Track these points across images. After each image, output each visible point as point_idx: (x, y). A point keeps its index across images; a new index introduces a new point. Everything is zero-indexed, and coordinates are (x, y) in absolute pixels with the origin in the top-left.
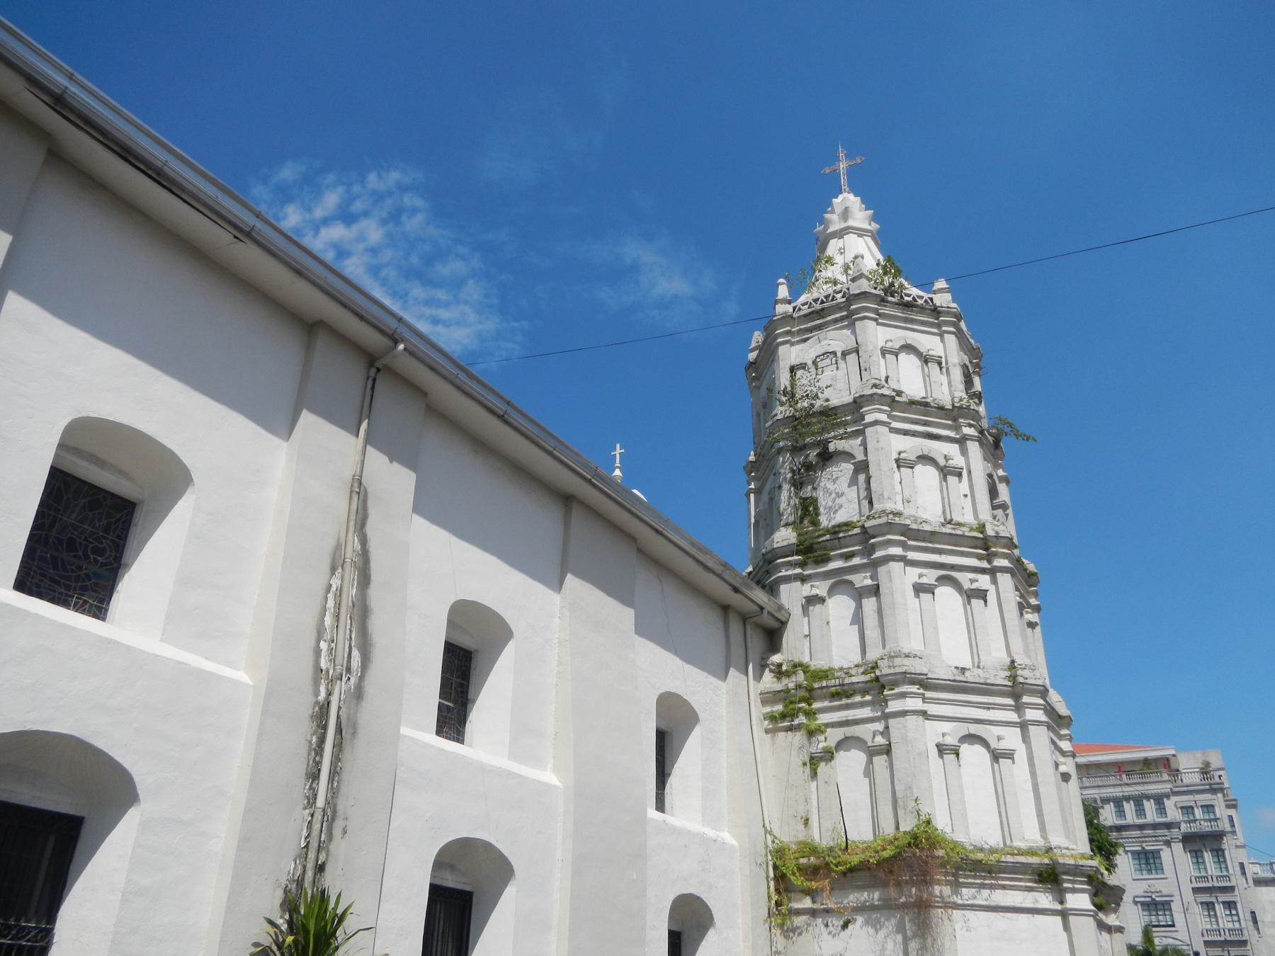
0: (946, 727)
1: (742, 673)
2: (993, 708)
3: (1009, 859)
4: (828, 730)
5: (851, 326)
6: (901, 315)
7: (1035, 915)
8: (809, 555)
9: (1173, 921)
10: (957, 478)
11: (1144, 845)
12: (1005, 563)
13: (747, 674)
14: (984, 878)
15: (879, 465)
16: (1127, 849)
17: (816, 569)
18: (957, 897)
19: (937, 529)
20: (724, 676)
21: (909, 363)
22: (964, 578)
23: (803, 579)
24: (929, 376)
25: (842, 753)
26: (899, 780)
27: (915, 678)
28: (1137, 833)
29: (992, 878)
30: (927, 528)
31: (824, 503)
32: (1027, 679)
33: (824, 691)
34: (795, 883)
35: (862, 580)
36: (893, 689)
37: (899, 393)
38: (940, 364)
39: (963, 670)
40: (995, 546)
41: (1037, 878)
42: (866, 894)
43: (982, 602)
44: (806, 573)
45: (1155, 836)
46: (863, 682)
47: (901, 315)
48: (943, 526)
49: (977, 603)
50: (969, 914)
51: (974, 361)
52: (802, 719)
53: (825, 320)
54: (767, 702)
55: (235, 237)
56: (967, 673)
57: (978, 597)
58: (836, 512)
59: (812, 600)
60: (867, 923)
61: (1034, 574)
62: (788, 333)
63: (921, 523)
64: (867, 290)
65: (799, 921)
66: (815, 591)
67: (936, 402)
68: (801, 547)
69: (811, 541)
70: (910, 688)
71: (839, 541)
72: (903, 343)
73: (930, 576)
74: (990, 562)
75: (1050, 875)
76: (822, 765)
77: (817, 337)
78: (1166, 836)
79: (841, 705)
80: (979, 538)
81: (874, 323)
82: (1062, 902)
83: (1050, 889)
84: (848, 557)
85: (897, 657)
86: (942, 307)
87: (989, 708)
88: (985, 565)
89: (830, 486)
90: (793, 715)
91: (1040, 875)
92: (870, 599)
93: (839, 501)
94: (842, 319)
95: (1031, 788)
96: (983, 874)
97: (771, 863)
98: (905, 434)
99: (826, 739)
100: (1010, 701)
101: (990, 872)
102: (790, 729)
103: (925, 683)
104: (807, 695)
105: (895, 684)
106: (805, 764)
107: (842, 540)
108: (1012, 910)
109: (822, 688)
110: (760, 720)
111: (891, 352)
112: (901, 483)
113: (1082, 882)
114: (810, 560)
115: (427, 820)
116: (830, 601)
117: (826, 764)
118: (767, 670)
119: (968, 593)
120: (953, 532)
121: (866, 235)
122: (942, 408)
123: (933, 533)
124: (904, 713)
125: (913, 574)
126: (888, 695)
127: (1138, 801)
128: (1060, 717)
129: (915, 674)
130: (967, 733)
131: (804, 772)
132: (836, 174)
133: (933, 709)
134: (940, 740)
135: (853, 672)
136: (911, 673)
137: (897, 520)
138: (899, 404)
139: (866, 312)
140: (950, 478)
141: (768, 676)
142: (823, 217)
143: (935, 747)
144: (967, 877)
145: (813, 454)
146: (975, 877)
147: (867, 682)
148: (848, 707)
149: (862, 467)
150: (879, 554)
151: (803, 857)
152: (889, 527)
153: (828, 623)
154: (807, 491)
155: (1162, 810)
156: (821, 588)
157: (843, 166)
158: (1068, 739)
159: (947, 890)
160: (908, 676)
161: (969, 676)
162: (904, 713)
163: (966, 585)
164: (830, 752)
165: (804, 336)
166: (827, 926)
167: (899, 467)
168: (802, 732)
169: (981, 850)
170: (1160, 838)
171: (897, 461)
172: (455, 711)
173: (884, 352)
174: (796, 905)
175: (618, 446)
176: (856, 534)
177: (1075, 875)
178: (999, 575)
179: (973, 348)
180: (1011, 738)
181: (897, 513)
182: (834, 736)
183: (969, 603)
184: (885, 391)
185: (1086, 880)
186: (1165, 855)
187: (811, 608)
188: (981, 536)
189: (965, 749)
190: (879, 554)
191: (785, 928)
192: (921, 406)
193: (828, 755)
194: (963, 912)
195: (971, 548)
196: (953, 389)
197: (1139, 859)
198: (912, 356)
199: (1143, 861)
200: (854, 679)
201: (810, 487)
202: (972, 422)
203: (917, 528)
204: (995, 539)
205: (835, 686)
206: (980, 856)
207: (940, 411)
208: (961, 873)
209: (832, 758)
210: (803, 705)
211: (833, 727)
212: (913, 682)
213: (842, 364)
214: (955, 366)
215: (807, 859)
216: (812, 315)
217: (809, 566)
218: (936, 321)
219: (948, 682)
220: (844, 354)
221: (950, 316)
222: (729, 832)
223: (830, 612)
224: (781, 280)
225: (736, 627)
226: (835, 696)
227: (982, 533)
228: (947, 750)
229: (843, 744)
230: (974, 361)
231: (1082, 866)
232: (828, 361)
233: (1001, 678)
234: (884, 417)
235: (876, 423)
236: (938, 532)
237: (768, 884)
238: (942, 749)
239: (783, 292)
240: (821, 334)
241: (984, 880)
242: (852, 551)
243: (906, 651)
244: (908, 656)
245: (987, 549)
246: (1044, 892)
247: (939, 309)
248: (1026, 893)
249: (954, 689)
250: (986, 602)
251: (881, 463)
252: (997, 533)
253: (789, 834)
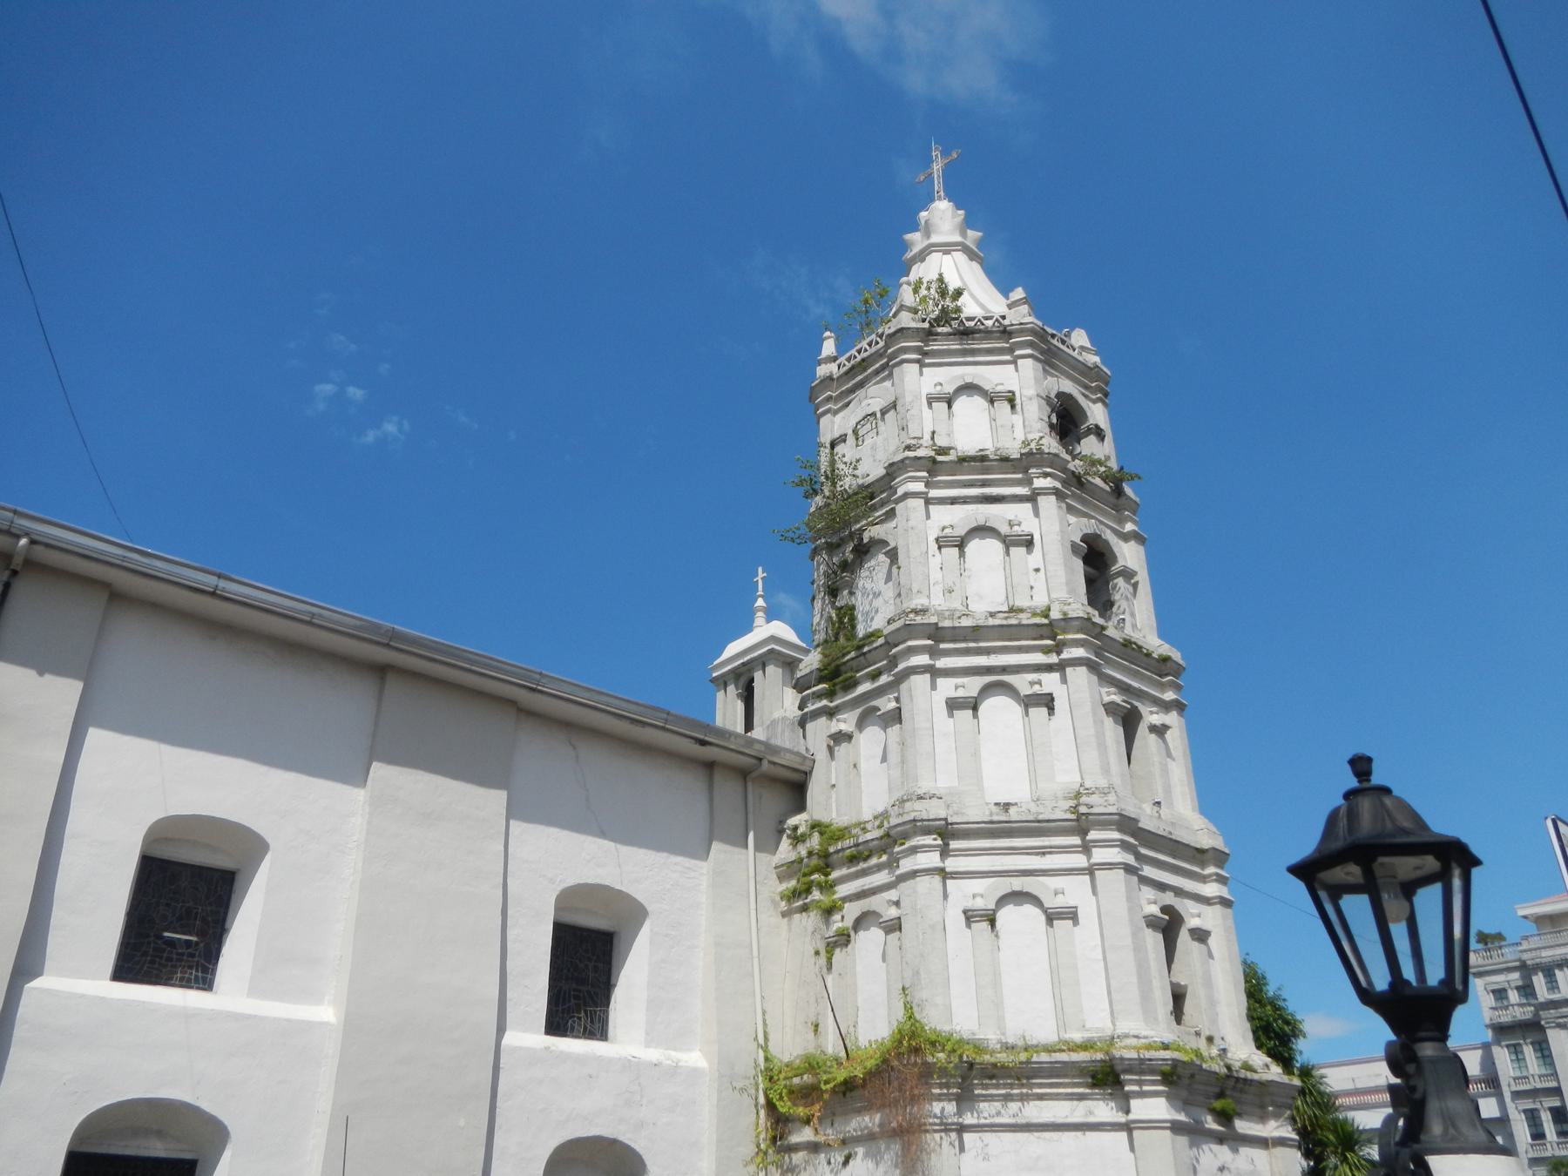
1: (734, 844)
2: (1050, 853)
3: (1044, 1057)
4: (846, 905)
5: (890, 375)
6: (958, 347)
7: (1087, 1133)
8: (837, 680)
10: (1024, 549)
12: (1079, 652)
13: (746, 846)
14: (1011, 1086)
15: (908, 551)
17: (843, 697)
18: (972, 1114)
19: (981, 622)
20: (704, 854)
21: (968, 406)
22: (1022, 682)
23: (831, 713)
24: (995, 420)
25: (861, 933)
26: (907, 963)
27: (929, 826)
29: (1022, 1086)
30: (966, 622)
31: (861, 609)
32: (1092, 807)
33: (841, 854)
34: (781, 1110)
35: (886, 704)
36: (904, 844)
37: (943, 451)
38: (1011, 401)
40: (1065, 632)
41: (1090, 1080)
42: (867, 1118)
43: (1045, 710)
44: (832, 705)
46: (877, 838)
47: (958, 347)
48: (991, 616)
49: (1039, 713)
50: (989, 1137)
51: (1093, 385)
52: (816, 895)
53: (866, 374)
54: (784, 876)
56: (1012, 810)
57: (1037, 705)
58: (872, 619)
59: (840, 738)
60: (866, 1155)
61: (1165, 660)
62: (829, 399)
63: (959, 618)
64: (903, 326)
65: (798, 1157)
66: (843, 727)
67: (998, 453)
68: (826, 672)
69: (838, 662)
70: (924, 840)
71: (865, 658)
72: (960, 383)
73: (973, 685)
74: (1059, 653)
75: (1107, 1074)
76: (838, 951)
77: (857, 399)
79: (858, 871)
80: (1043, 625)
81: (917, 366)
82: (1128, 1112)
83: (1111, 1094)
84: (875, 676)
85: (908, 800)
86: (1012, 325)
87: (1044, 854)
88: (1053, 659)
89: (868, 585)
90: (808, 891)
91: (1093, 1077)
92: (894, 728)
93: (877, 603)
94: (883, 368)
95: (1101, 957)
96: (1009, 1081)
97: (761, 1086)
98: (952, 504)
99: (843, 917)
100: (1076, 840)
101: (1019, 1079)
102: (805, 909)
103: (946, 832)
104: (821, 863)
105: (906, 836)
106: (817, 953)
107: (867, 656)
108: (1051, 1128)
109: (837, 852)
110: (773, 901)
111: (938, 399)
112: (941, 568)
113: (1153, 1083)
114: (837, 687)
115: (65, 1084)
116: (862, 735)
117: (841, 951)
118: (785, 837)
119: (1025, 700)
120: (1004, 622)
121: (954, 250)
122: (1005, 460)
123: (976, 629)
124: (914, 874)
125: (947, 687)
126: (898, 853)
128: (1201, 851)
129: (929, 820)
130: (1009, 891)
131: (815, 964)
133: (952, 864)
134: (970, 904)
135: (869, 826)
136: (922, 820)
137: (919, 620)
138: (944, 465)
139: (905, 353)
140: (1013, 550)
141: (785, 843)
142: (903, 240)
143: (963, 915)
144: (986, 1087)
145: (848, 552)
146: (997, 1086)
147: (882, 838)
148: (864, 873)
149: (893, 555)
150: (901, 666)
151: (795, 1076)
152: (910, 630)
153: (855, 766)
154: (843, 599)
156: (846, 722)
157: (937, 167)
158: (1216, 881)
159: (951, 1108)
160: (918, 824)
161: (1014, 814)
162: (914, 874)
163: (1025, 690)
164: (843, 935)
165: (844, 399)
166: (829, 1163)
167: (940, 548)
168: (815, 912)
169: (1009, 1048)
171: (937, 540)
172: (202, 945)
173: (931, 400)
174: (795, 1139)
175: (760, 569)
176: (881, 646)
177: (1142, 1073)
178: (1069, 670)
179: (1089, 367)
180: (1075, 891)
181: (921, 611)
182: (852, 911)
183: (1027, 714)
184: (921, 453)
185: (1159, 1078)
187: (837, 748)
188: (1045, 621)
189: (1007, 915)
190: (901, 666)
191: (785, 1167)
192: (979, 461)
193: (843, 939)
194: (980, 1134)
195: (1035, 639)
196: (1028, 429)
198: (976, 397)
200: (869, 836)
201: (845, 592)
202: (1049, 470)
203: (951, 625)
204: (1063, 623)
205: (850, 848)
206: (1002, 1057)
207: (1005, 464)
208: (976, 1082)
209: (848, 942)
210: (815, 876)
211: (850, 901)
212: (927, 831)
213: (882, 427)
214: (1031, 399)
215: (799, 1078)
216: (856, 370)
217: (839, 695)
218: (1008, 345)
219: (983, 825)
220: (884, 412)
221: (1026, 334)
222: (700, 1050)
223: (862, 752)
224: (827, 334)
226: (853, 860)
227: (1047, 616)
228: (976, 916)
229: (860, 922)
230: (1093, 385)
231: (1150, 1060)
232: (869, 426)
233: (1061, 812)
234: (919, 487)
235: (906, 496)
236: (981, 627)
237: (757, 1113)
238: (970, 916)
239: (829, 348)
240: (861, 393)
241: (1012, 1088)
242: (878, 668)
243: (920, 792)
244: (921, 798)
245: (1054, 640)
246: (1104, 1099)
247: (1008, 328)
248: (1075, 1103)
249: (992, 833)
250: (1051, 709)
251: (910, 547)
252: (1065, 614)
253: (790, 1046)
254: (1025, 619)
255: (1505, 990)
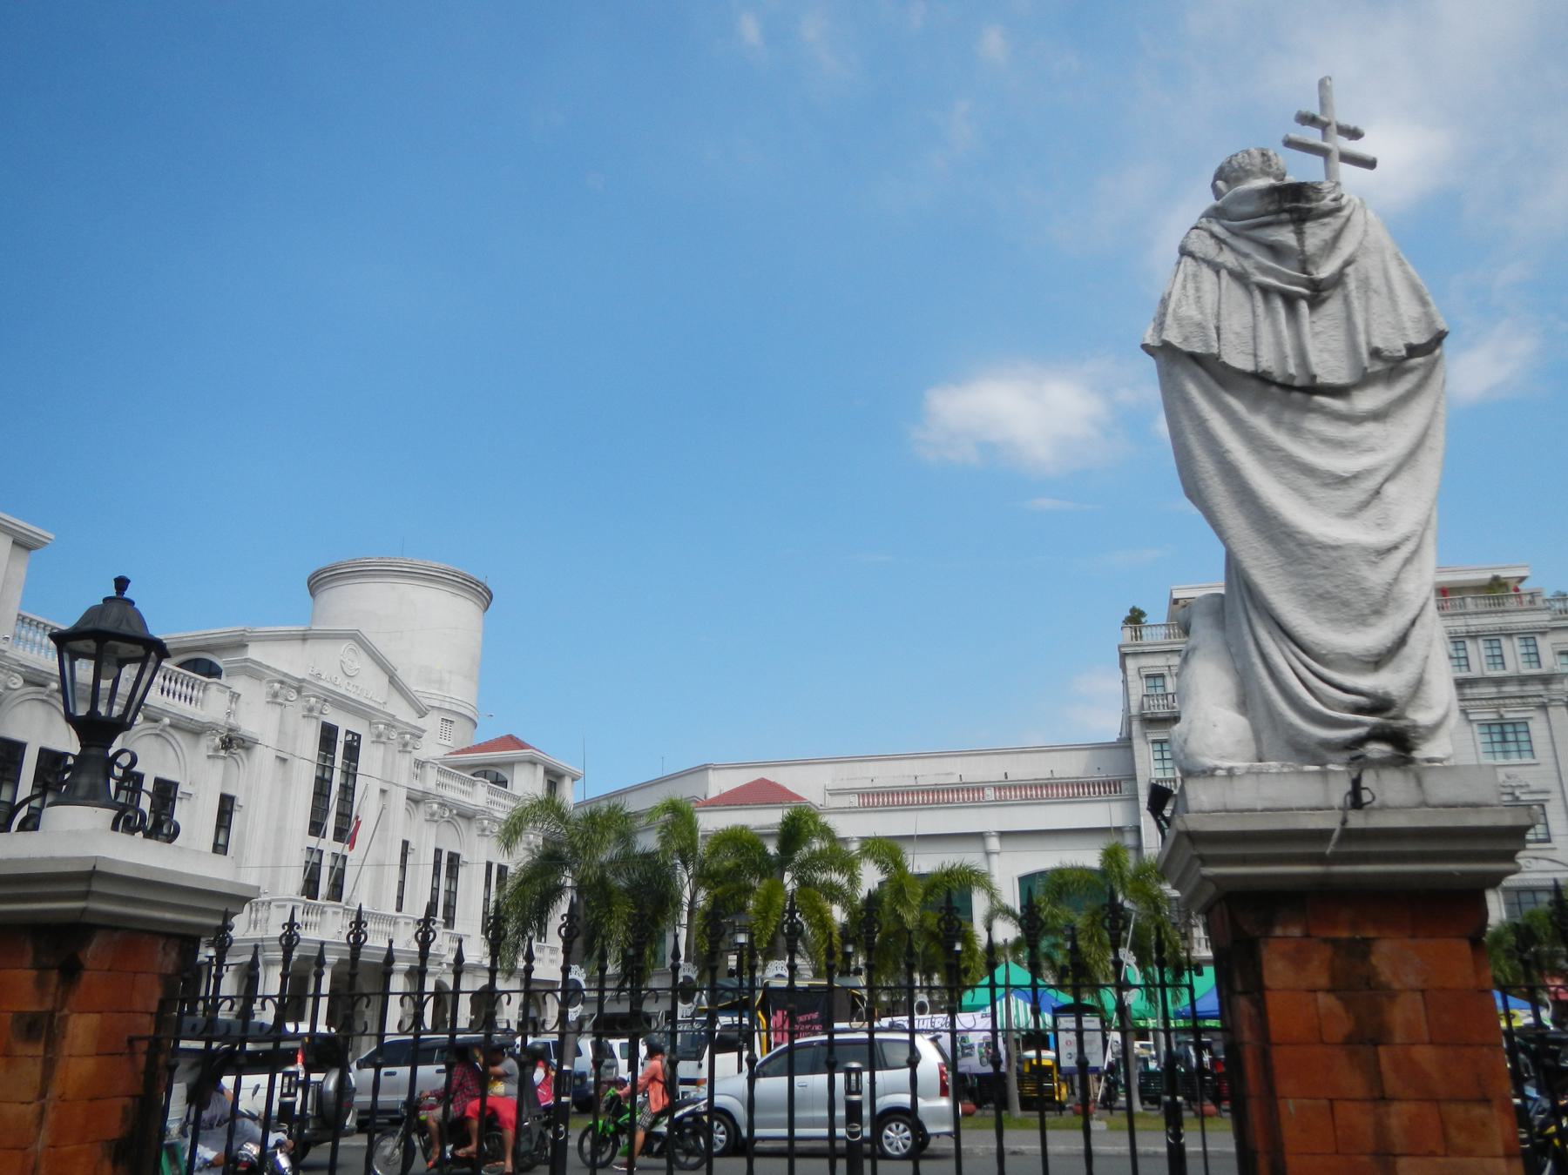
9: (1548, 834)
11: (1503, 710)
16: (1472, 717)
28: (1491, 691)
45: (1522, 697)
78: (1541, 696)
127: (1493, 638)
155: (1534, 657)
170: (1530, 700)
186: (1538, 727)
197: (1490, 733)
199: (1497, 738)
255: (1162, 676)
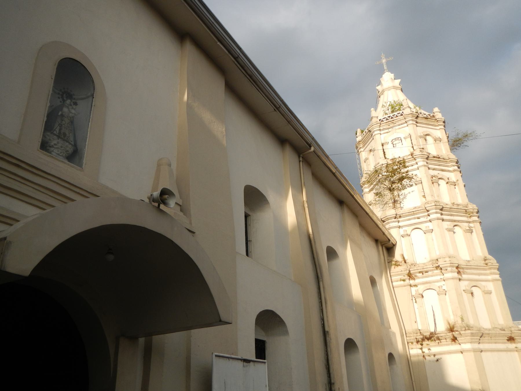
0: (466, 283)
39: (469, 261)
55: (274, 110)
56: (471, 262)
132: (382, 65)
220: (405, 138)
225: (380, 248)
232: (397, 142)
254: (460, 207)
